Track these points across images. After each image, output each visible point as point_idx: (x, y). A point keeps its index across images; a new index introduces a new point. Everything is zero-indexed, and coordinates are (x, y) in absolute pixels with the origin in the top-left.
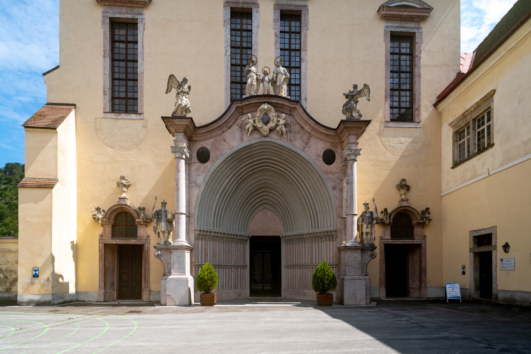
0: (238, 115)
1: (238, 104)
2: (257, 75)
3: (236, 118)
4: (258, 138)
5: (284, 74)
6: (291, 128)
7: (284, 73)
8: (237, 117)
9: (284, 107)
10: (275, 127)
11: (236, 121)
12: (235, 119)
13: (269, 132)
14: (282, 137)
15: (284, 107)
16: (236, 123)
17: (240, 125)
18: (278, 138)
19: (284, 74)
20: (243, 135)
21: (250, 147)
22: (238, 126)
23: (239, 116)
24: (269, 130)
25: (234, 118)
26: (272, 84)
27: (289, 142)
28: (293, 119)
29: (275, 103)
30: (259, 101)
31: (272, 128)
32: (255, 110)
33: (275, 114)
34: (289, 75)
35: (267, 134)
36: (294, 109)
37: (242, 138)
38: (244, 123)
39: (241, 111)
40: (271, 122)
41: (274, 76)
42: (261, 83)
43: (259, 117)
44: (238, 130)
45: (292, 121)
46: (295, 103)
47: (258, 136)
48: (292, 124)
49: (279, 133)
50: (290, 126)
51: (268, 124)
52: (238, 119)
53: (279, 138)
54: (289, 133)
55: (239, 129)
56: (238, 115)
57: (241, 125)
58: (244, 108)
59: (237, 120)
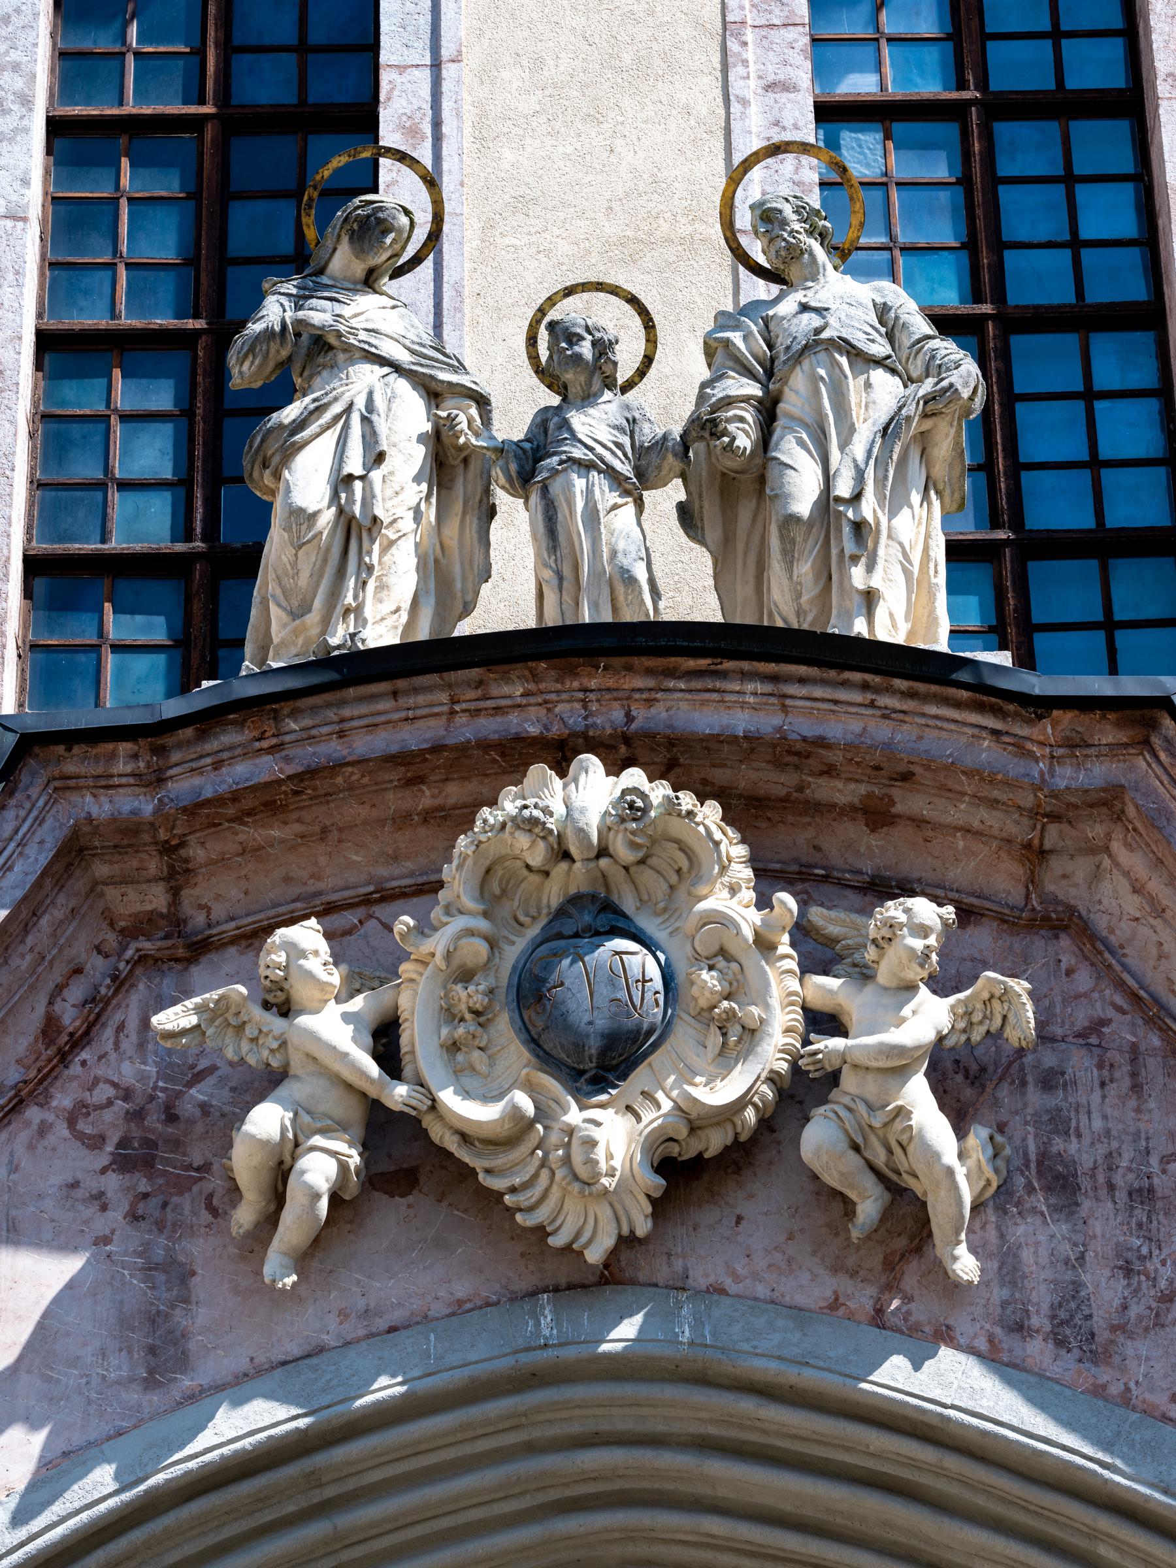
0: (97, 966)
1: (104, 784)
2: (433, 393)
3: (69, 1016)
4: (459, 1309)
5: (879, 362)
6: (1058, 1123)
7: (880, 348)
8: (76, 993)
9: (908, 802)
10: (766, 1124)
11: (63, 1057)
12: (50, 1027)
13: (660, 1206)
14: (910, 1281)
15: (908, 802)
16: (63, 1099)
17: (137, 1116)
18: (835, 1305)
19: (879, 362)
20: (185, 1275)
21: (313, 1480)
22: (95, 1142)
23: (120, 983)
24: (665, 1166)
25: (33, 1018)
26: (687, 515)
27: (1037, 1350)
28: (1084, 979)
29: (750, 744)
30: (466, 730)
31: (715, 1142)
32: (397, 875)
33: (763, 902)
34: (969, 369)
35: (627, 1241)
36: (1095, 830)
37: (154, 1319)
38: (197, 1093)
39: (157, 899)
40: (683, 1037)
41: (717, 392)
42: (503, 499)
43: (466, 976)
44: (100, 1200)
45: (1081, 1017)
46: (1107, 734)
47: (461, 1289)
48: (1080, 1064)
49: (848, 1208)
50: (1035, 1098)
51: (640, 1077)
52: (108, 1034)
53: (862, 1298)
54: (1039, 1201)
55: (113, 1182)
56: (97, 966)
57: (154, 1120)
58: (197, 853)
59: (80, 1040)
